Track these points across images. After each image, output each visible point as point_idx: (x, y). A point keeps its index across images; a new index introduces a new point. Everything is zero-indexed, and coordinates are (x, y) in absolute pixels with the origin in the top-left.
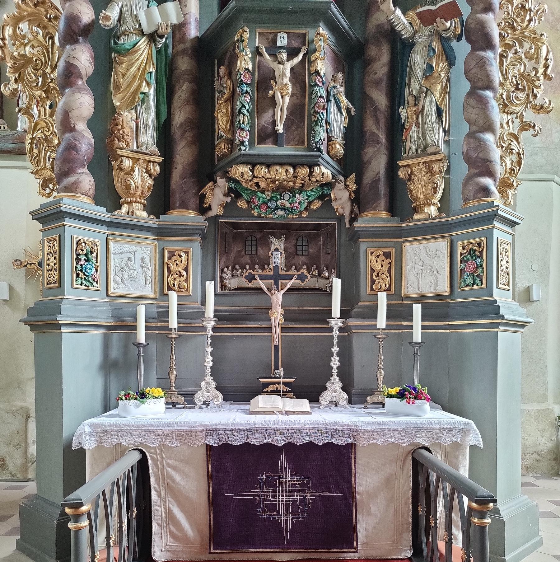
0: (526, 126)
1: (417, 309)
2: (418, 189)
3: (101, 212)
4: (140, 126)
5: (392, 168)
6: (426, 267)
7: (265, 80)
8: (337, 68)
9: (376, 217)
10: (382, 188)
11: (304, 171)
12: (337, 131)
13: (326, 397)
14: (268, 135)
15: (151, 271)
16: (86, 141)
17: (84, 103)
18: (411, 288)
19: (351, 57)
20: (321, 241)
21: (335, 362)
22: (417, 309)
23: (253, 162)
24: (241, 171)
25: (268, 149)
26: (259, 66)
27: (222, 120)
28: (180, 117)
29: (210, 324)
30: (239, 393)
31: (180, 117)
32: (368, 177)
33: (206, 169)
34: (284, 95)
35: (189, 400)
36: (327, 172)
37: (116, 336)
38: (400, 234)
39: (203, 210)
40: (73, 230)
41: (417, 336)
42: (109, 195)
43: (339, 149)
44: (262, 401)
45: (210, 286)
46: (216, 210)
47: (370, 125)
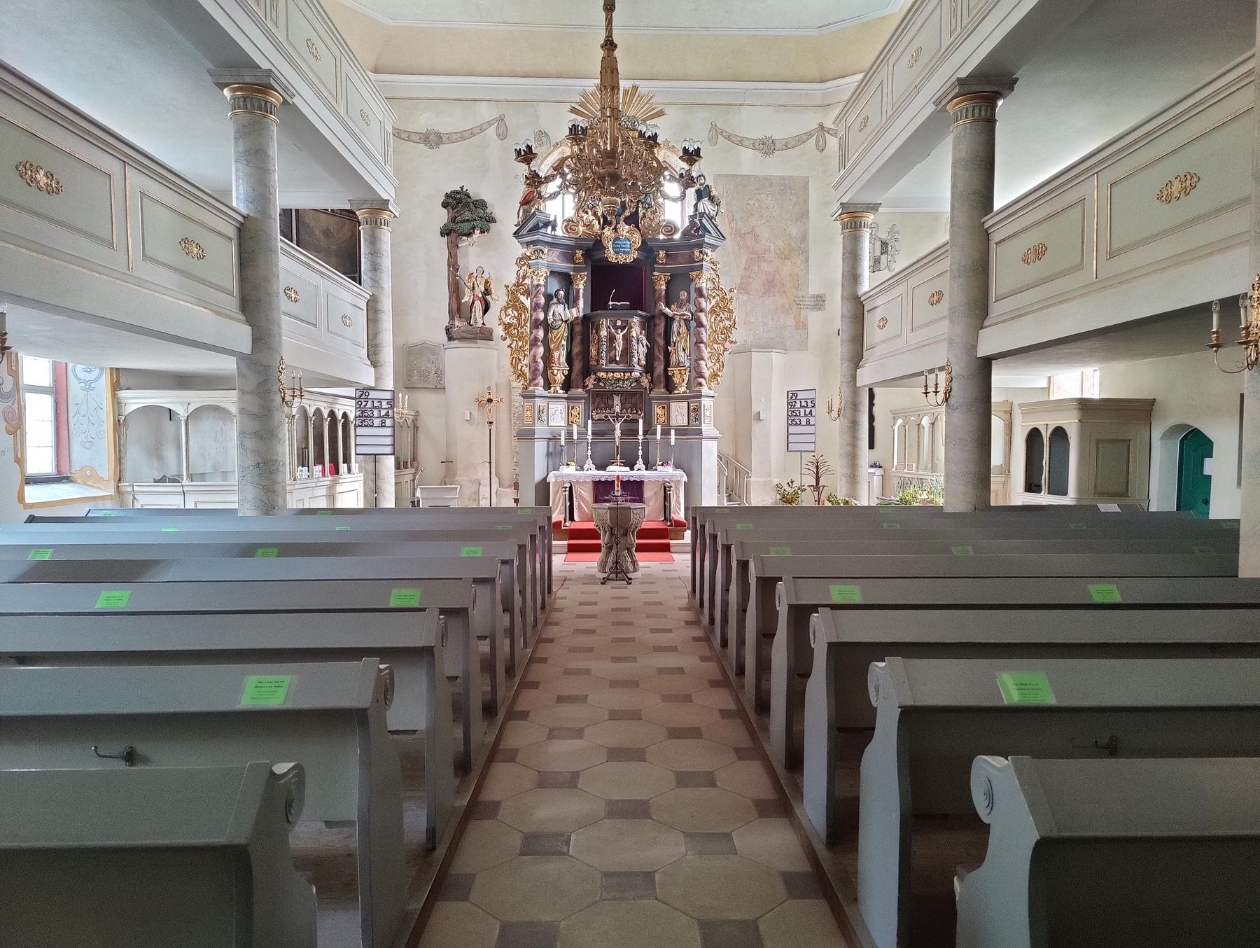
0: (725, 350)
1: (673, 432)
2: (676, 380)
3: (546, 393)
4: (560, 355)
5: (666, 371)
6: (679, 413)
7: (612, 339)
8: (643, 328)
9: (660, 391)
10: (663, 379)
12: (642, 357)
13: (636, 467)
14: (612, 360)
15: (564, 415)
17: (541, 350)
18: (673, 422)
19: (648, 325)
20: (636, 400)
21: (640, 453)
22: (673, 432)
23: (607, 371)
24: (601, 374)
25: (613, 366)
26: (610, 333)
27: (593, 352)
28: (576, 350)
29: (590, 437)
31: (576, 350)
32: (656, 374)
33: (587, 371)
34: (619, 344)
35: (582, 469)
36: (637, 374)
37: (551, 443)
38: (669, 399)
39: (584, 387)
40: (539, 402)
42: (548, 385)
43: (644, 363)
44: (610, 468)
45: (590, 422)
46: (590, 386)
47: (656, 352)
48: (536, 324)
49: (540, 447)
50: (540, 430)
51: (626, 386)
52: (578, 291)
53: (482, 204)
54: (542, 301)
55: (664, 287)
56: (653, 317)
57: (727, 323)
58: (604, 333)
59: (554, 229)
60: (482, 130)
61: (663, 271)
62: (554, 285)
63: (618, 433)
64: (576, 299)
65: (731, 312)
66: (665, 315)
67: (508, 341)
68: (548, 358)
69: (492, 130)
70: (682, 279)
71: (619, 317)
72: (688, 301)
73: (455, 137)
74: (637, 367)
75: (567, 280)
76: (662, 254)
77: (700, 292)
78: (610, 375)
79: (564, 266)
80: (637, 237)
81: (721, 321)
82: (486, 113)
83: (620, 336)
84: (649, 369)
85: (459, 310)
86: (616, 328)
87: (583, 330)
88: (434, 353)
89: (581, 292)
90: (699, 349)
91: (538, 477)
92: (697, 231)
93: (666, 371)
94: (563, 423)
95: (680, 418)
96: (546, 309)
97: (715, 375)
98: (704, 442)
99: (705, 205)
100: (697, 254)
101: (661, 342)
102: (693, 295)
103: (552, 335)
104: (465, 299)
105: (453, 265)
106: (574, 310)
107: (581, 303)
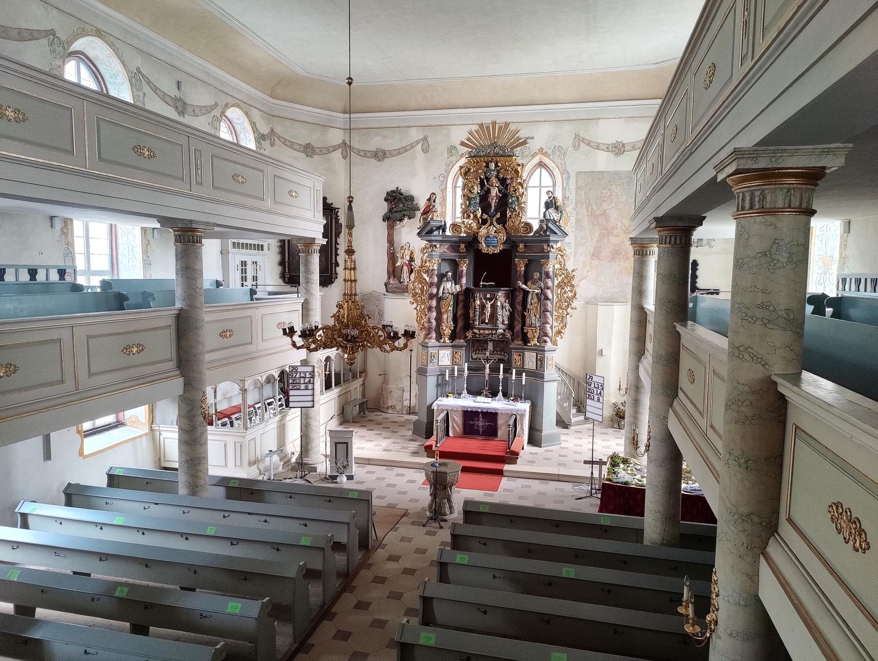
1: (524, 374)
5: (522, 329)
7: (483, 307)
9: (518, 343)
10: (520, 335)
11: (494, 332)
12: (506, 319)
14: (483, 322)
16: (434, 323)
17: (434, 314)
18: (526, 367)
19: (511, 297)
20: (502, 345)
21: (501, 388)
22: (524, 374)
23: (479, 329)
24: (476, 331)
26: (482, 303)
27: (471, 315)
28: (459, 313)
30: (475, 392)
31: (459, 313)
32: (515, 330)
41: (524, 383)
42: (439, 336)
43: (506, 322)
44: (480, 399)
48: (431, 296)
49: (431, 381)
50: (431, 367)
51: (495, 337)
52: (462, 271)
53: (411, 198)
54: (436, 279)
55: (523, 269)
56: (515, 289)
57: (570, 294)
58: (478, 302)
59: (444, 231)
60: (412, 147)
61: (523, 257)
62: (446, 268)
63: (487, 371)
64: (461, 277)
65: (573, 286)
66: (524, 290)
67: (415, 305)
68: (439, 319)
69: (419, 146)
70: (536, 264)
71: (489, 292)
72: (540, 279)
73: (394, 153)
74: (501, 326)
75: (454, 265)
76: (521, 246)
77: (547, 275)
78: (482, 332)
79: (452, 255)
80: (503, 237)
81: (565, 292)
82: (415, 135)
83: (489, 305)
84: (511, 327)
85: (394, 271)
86: (486, 299)
87: (464, 299)
88: (378, 300)
89: (465, 272)
90: (545, 316)
91: (428, 402)
92: (545, 232)
93: (522, 329)
94: (449, 363)
95: (531, 364)
96: (438, 286)
97: (559, 332)
98: (545, 384)
99: (553, 214)
100: (546, 247)
101: (519, 308)
102: (544, 276)
103: (443, 303)
104: (398, 264)
105: (391, 241)
106: (458, 287)
107: (464, 280)
